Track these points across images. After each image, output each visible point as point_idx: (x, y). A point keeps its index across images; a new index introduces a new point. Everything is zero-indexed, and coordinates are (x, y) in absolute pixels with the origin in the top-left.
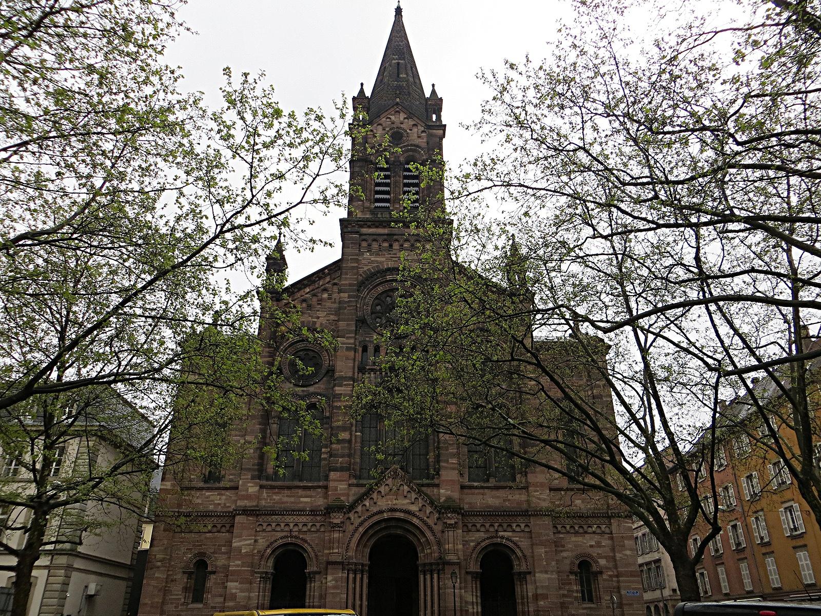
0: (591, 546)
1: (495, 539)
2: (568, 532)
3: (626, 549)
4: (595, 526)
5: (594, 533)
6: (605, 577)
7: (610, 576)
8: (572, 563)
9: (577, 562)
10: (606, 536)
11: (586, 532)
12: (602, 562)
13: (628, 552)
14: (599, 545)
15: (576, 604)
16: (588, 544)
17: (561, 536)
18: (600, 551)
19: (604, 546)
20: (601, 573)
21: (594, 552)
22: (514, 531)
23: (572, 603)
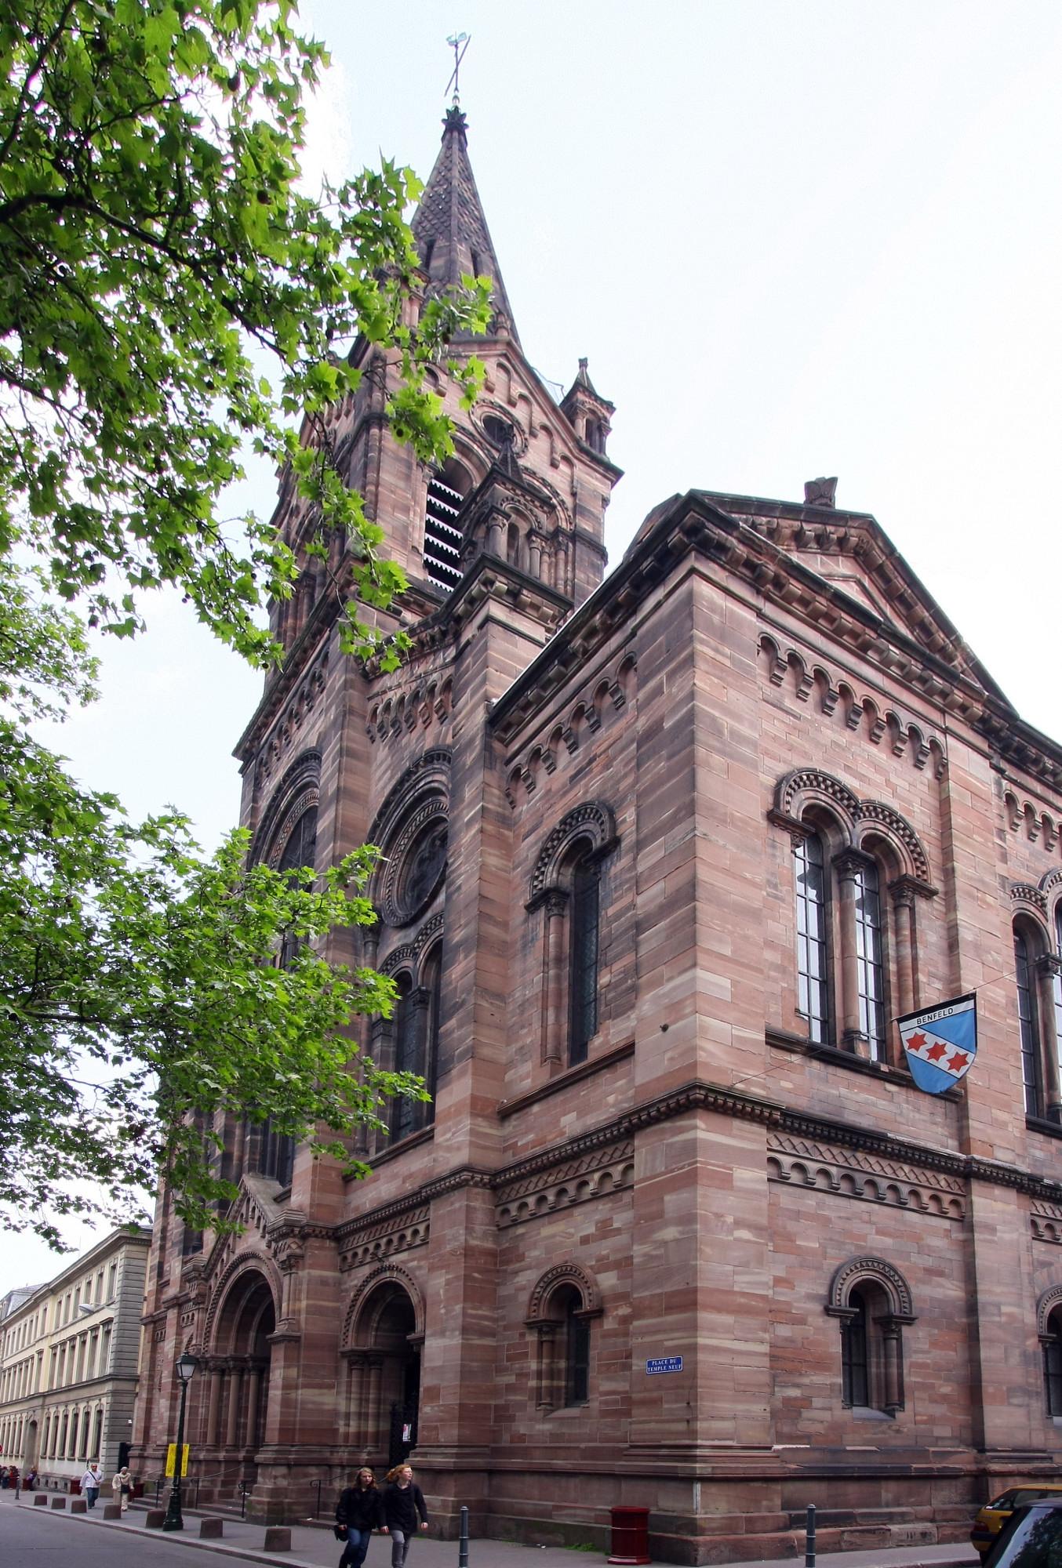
0: (585, 1240)
1: (383, 1276)
2: (534, 1217)
3: (666, 1224)
4: (597, 1176)
5: (596, 1197)
6: (609, 1324)
7: (625, 1320)
8: (536, 1301)
9: (547, 1295)
10: (626, 1197)
11: (575, 1204)
12: (608, 1281)
13: (670, 1233)
14: (605, 1230)
15: (531, 1408)
16: (577, 1238)
17: (521, 1230)
18: (605, 1248)
19: (618, 1231)
20: (599, 1313)
21: (587, 1257)
22: (410, 1247)
23: (522, 1406)
